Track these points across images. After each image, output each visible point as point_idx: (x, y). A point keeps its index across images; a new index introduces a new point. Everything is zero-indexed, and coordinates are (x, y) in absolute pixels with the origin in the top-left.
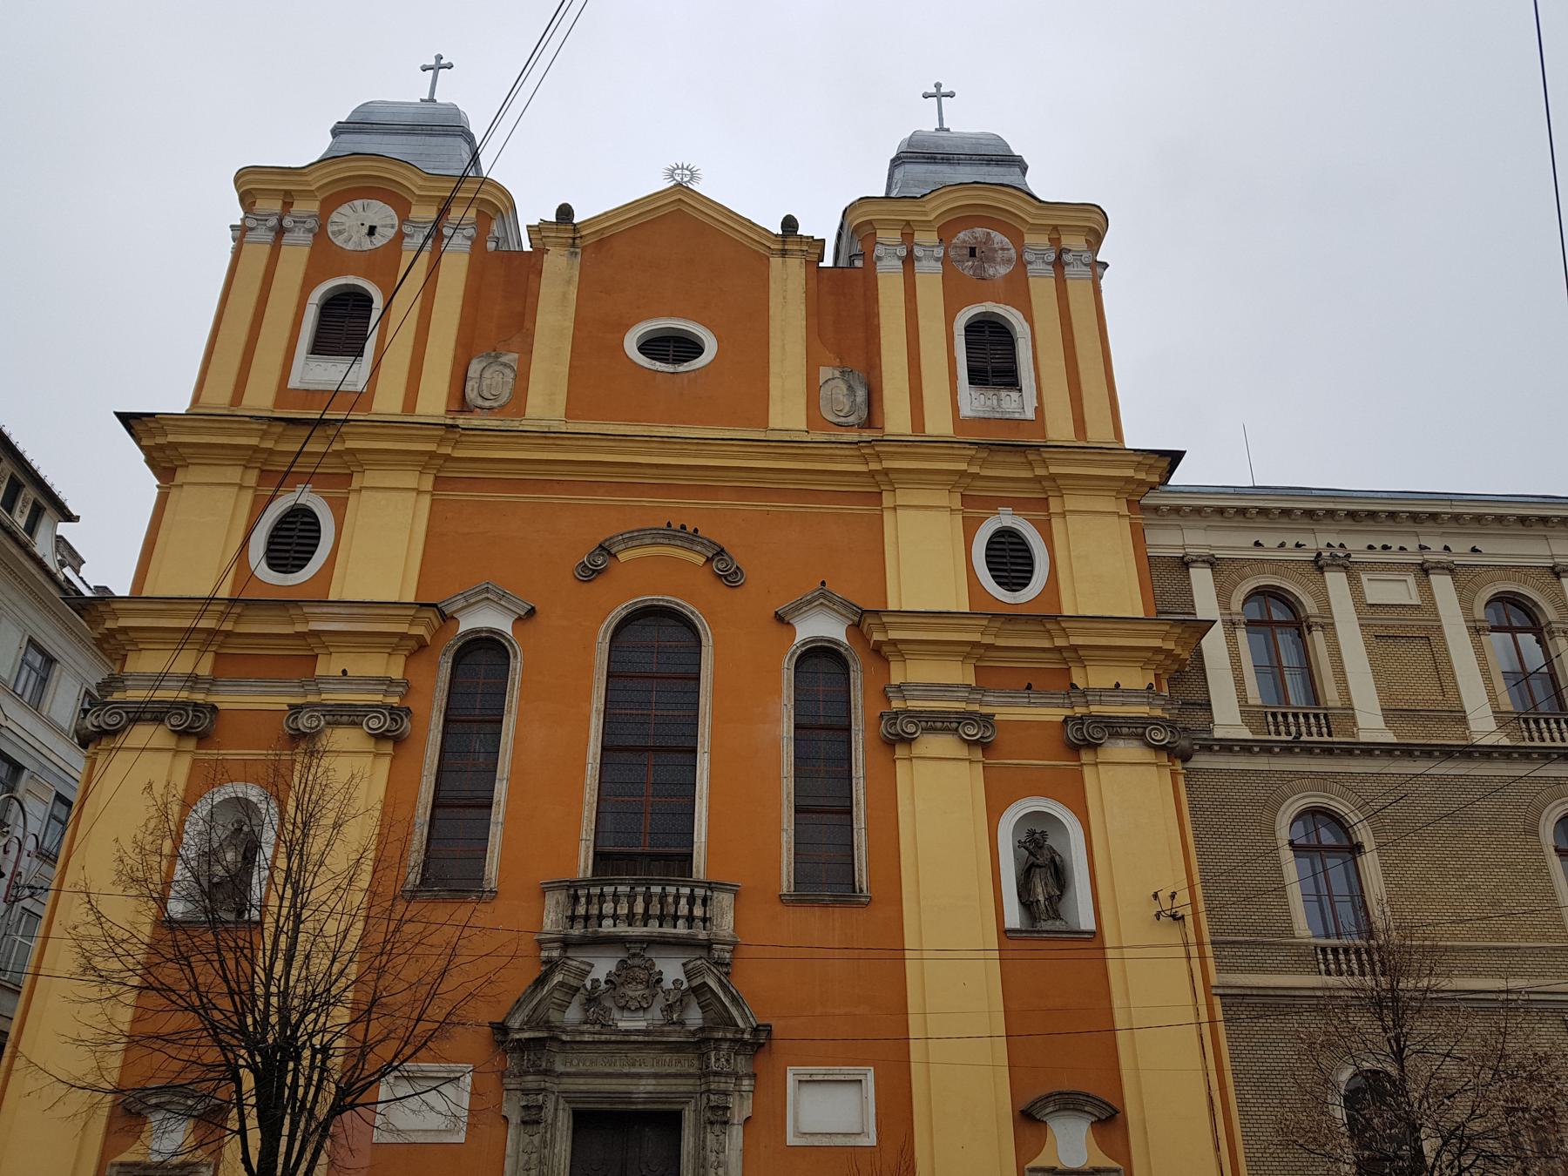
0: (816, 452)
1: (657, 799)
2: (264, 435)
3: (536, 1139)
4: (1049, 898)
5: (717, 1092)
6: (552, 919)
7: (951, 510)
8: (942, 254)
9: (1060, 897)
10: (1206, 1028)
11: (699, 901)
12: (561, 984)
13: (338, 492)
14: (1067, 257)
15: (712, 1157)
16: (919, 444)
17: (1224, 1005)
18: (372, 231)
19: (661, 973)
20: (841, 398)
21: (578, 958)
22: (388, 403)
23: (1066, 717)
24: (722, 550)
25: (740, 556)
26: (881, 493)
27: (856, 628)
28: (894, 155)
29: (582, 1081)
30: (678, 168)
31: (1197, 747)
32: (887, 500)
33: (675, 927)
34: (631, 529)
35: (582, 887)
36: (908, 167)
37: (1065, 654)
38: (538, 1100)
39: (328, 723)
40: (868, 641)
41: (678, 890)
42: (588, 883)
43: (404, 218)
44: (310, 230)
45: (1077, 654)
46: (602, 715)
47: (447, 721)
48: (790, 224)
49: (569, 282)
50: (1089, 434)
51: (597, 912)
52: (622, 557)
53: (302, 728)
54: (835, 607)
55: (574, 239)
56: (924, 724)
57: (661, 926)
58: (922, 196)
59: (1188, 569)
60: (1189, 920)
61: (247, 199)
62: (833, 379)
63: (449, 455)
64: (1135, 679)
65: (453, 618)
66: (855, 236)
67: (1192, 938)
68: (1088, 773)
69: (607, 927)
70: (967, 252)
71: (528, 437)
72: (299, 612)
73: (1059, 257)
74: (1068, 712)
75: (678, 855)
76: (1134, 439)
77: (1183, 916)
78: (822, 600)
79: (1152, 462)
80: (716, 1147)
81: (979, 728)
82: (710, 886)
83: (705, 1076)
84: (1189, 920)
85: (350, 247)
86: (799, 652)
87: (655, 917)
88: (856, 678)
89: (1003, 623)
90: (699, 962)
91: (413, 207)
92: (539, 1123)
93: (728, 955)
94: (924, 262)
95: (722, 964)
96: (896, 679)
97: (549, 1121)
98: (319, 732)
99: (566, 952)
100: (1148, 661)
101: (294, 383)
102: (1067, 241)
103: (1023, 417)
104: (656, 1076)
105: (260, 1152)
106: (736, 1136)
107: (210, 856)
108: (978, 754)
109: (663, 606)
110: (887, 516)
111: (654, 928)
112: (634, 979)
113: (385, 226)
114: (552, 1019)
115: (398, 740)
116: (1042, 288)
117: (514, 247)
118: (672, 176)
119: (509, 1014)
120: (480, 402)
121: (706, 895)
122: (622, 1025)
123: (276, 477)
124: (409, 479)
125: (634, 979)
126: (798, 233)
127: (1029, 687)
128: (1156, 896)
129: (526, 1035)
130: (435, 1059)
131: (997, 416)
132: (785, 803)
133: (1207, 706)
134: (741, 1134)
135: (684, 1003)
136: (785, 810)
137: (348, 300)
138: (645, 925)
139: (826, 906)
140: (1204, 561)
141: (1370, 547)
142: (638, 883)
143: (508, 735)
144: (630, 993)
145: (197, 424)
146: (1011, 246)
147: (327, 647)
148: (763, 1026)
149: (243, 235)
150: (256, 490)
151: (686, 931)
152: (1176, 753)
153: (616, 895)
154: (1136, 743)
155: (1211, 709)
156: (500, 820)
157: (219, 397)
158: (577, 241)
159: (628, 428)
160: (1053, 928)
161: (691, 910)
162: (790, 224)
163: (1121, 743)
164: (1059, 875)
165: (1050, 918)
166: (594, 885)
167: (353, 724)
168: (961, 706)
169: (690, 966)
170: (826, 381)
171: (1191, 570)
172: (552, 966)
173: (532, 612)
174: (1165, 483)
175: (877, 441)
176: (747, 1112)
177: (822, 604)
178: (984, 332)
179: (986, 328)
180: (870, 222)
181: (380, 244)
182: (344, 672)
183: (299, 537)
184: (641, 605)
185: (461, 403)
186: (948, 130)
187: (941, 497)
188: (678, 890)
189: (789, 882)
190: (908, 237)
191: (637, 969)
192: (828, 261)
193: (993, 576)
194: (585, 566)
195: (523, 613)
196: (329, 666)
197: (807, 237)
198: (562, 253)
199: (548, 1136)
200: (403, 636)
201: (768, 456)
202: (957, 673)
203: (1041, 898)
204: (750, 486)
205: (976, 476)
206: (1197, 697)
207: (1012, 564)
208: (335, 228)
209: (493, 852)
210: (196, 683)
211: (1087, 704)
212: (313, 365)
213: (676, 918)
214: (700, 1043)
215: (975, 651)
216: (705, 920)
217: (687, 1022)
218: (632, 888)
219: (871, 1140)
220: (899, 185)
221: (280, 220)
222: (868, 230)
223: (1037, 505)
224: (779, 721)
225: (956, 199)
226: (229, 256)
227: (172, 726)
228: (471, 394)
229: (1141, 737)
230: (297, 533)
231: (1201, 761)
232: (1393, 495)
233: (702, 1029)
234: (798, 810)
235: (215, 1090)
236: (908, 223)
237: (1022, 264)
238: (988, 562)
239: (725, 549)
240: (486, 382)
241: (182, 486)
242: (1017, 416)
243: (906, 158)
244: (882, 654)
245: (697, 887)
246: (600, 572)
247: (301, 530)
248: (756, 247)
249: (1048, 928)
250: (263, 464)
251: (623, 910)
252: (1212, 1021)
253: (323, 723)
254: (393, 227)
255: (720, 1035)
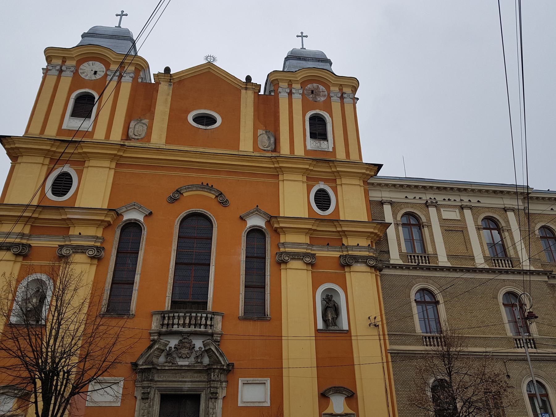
0: (256, 159)
1: (195, 282)
2: (52, 145)
3: (147, 405)
4: (333, 318)
5: (214, 387)
6: (155, 325)
7: (303, 182)
8: (302, 92)
9: (336, 318)
10: (385, 364)
11: (209, 319)
12: (158, 348)
13: (80, 168)
14: (345, 96)
15: (211, 411)
16: (292, 158)
17: (391, 356)
18: (95, 73)
19: (194, 345)
20: (265, 141)
21: (164, 339)
22: (100, 135)
23: (341, 255)
24: (222, 193)
25: (228, 196)
26: (278, 175)
27: (268, 222)
28: (286, 56)
29: (164, 383)
30: (209, 56)
31: (384, 267)
32: (281, 177)
33: (200, 328)
34: (188, 185)
35: (166, 313)
36: (291, 61)
37: (341, 233)
38: (148, 391)
39: (73, 252)
40: (273, 227)
41: (202, 315)
42: (169, 312)
43: (108, 69)
44: (72, 71)
45: (345, 234)
46: (176, 252)
47: (118, 252)
48: (249, 78)
49: (168, 95)
50: (351, 157)
51: (172, 323)
52: (185, 194)
53: (63, 254)
54: (261, 215)
55: (170, 79)
56: (291, 257)
57: (195, 328)
58: (295, 71)
59: (383, 205)
60: (380, 326)
61: (49, 59)
62: (263, 134)
63: (122, 155)
64: (364, 242)
65: (121, 215)
66: (272, 84)
67: (381, 333)
68: (347, 275)
69: (175, 328)
70: (310, 92)
71: (151, 150)
72: (63, 211)
73: (342, 95)
74: (341, 254)
75: (202, 302)
76: (366, 159)
77: (378, 325)
78: (257, 212)
79: (372, 168)
80: (212, 407)
81: (310, 259)
82: (213, 313)
83: (209, 381)
84: (380, 326)
85: (87, 78)
86: (248, 230)
87: (193, 324)
88: (268, 240)
89: (320, 222)
90: (208, 341)
91: (111, 65)
92: (148, 399)
93: (219, 338)
94: (296, 95)
95: (217, 342)
96: (282, 241)
97: (152, 398)
98: (70, 256)
99: (160, 337)
100: (369, 237)
101: (64, 127)
102: (345, 90)
103: (328, 150)
104: (191, 382)
105: (42, 410)
106: (220, 403)
107: (26, 300)
108: (310, 268)
109: (200, 213)
110: (281, 183)
111: (192, 328)
112: (185, 347)
113: (100, 71)
114: (154, 361)
115: (99, 259)
116: (336, 106)
117: (148, 81)
118: (207, 59)
119: (138, 359)
120: (134, 137)
122: (180, 363)
123: (56, 161)
124: (107, 164)
125: (185, 347)
126: (252, 82)
127: (328, 244)
128: (369, 318)
129: (144, 367)
130: (110, 376)
131: (320, 149)
132: (241, 284)
133: (388, 252)
134: (222, 403)
135: (202, 356)
136: (241, 287)
137: (86, 98)
138: (189, 327)
139: (255, 321)
140: (388, 203)
141: (444, 199)
142: (187, 312)
143: (141, 258)
144: (183, 352)
145: (26, 141)
146: (326, 91)
147: (74, 224)
148: (231, 364)
149: (47, 72)
150: (48, 166)
151: (204, 330)
152: (377, 269)
153: (179, 317)
154: (364, 265)
155: (389, 254)
156: (137, 289)
157: (36, 131)
158: (172, 80)
159: (188, 148)
160: (334, 329)
161: (206, 322)
162: (249, 78)
163: (359, 265)
164: (336, 310)
165: (333, 325)
166: (171, 313)
167: (83, 253)
168: (304, 251)
169: (205, 342)
170: (260, 135)
171: (384, 205)
172: (154, 342)
173: (151, 213)
174: (376, 175)
175: (278, 156)
176: (224, 394)
177: (257, 213)
178: (315, 120)
179: (316, 119)
180: (277, 79)
181: (98, 78)
182: (80, 234)
183: (65, 184)
184: (191, 212)
185: (127, 137)
186: (305, 49)
187: (300, 177)
188: (202, 315)
189: (242, 312)
190: (290, 86)
191: (186, 343)
192: (262, 92)
193: (317, 206)
194: (171, 197)
195: (147, 214)
196: (75, 231)
197: (255, 84)
198: (166, 84)
199: (151, 403)
200: (102, 221)
201: (239, 160)
202: (303, 239)
203: (330, 318)
204: (232, 171)
205: (312, 170)
206: (385, 249)
207: (323, 201)
208: (82, 71)
209: (133, 300)
210: (24, 236)
211: (348, 251)
212: (72, 120)
213: (200, 325)
214: (208, 370)
215: (310, 231)
217: (203, 362)
218: (185, 314)
219: (268, 404)
220: (287, 67)
221: (61, 67)
222: (276, 82)
223: (332, 181)
224: (240, 254)
225: (307, 73)
226: (41, 79)
227: (14, 252)
228: (131, 134)
229: (366, 263)
230: (63, 182)
231: (386, 272)
232: (452, 182)
233: (209, 365)
234: (246, 287)
235: (26, 387)
236: (290, 80)
237: (329, 97)
238: (315, 201)
239: (223, 193)
240: (136, 129)
241: (20, 163)
242: (326, 150)
243: (290, 57)
244: (277, 232)
245: (209, 314)
246: (176, 200)
247: (65, 181)
248: (236, 86)
249: (332, 329)
250: (51, 156)
251: (181, 322)
252: (387, 362)
253: (71, 252)
254: (103, 72)
255: (215, 367)
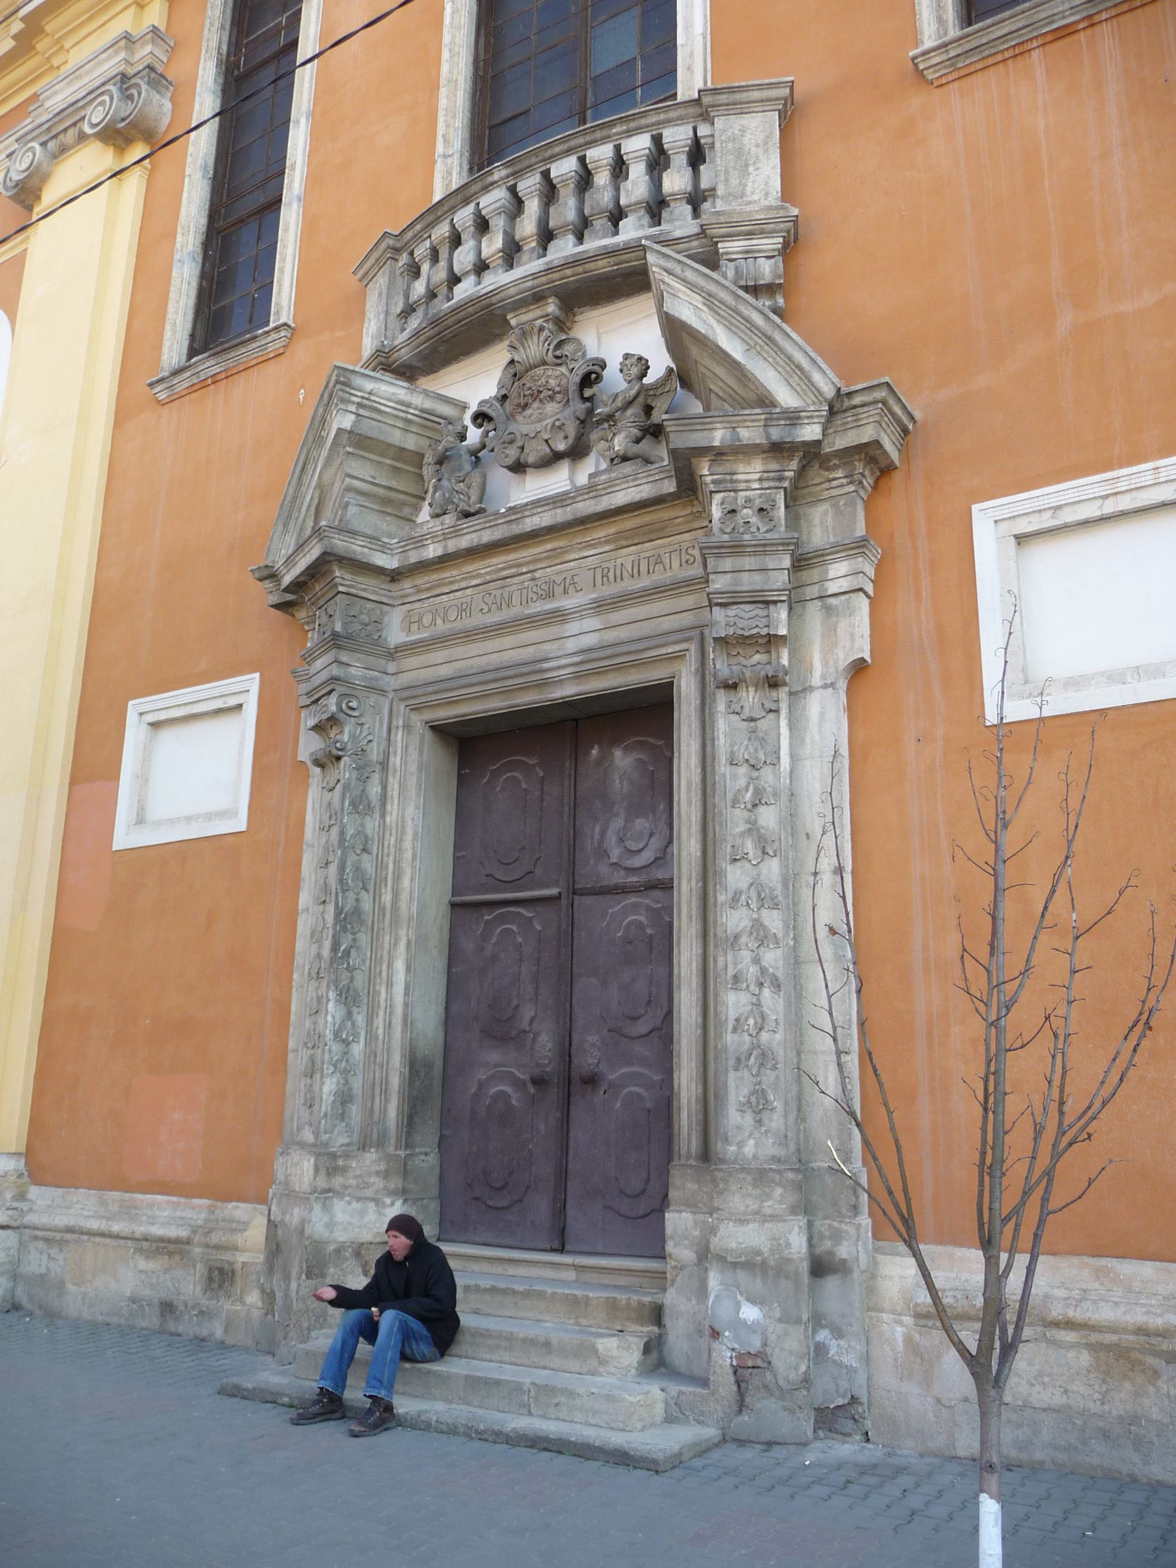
29: (439, 656)
121: (696, 139)
125: (536, 395)
144: (525, 429)
191: (539, 371)
216: (696, 199)
251: (493, 245)
